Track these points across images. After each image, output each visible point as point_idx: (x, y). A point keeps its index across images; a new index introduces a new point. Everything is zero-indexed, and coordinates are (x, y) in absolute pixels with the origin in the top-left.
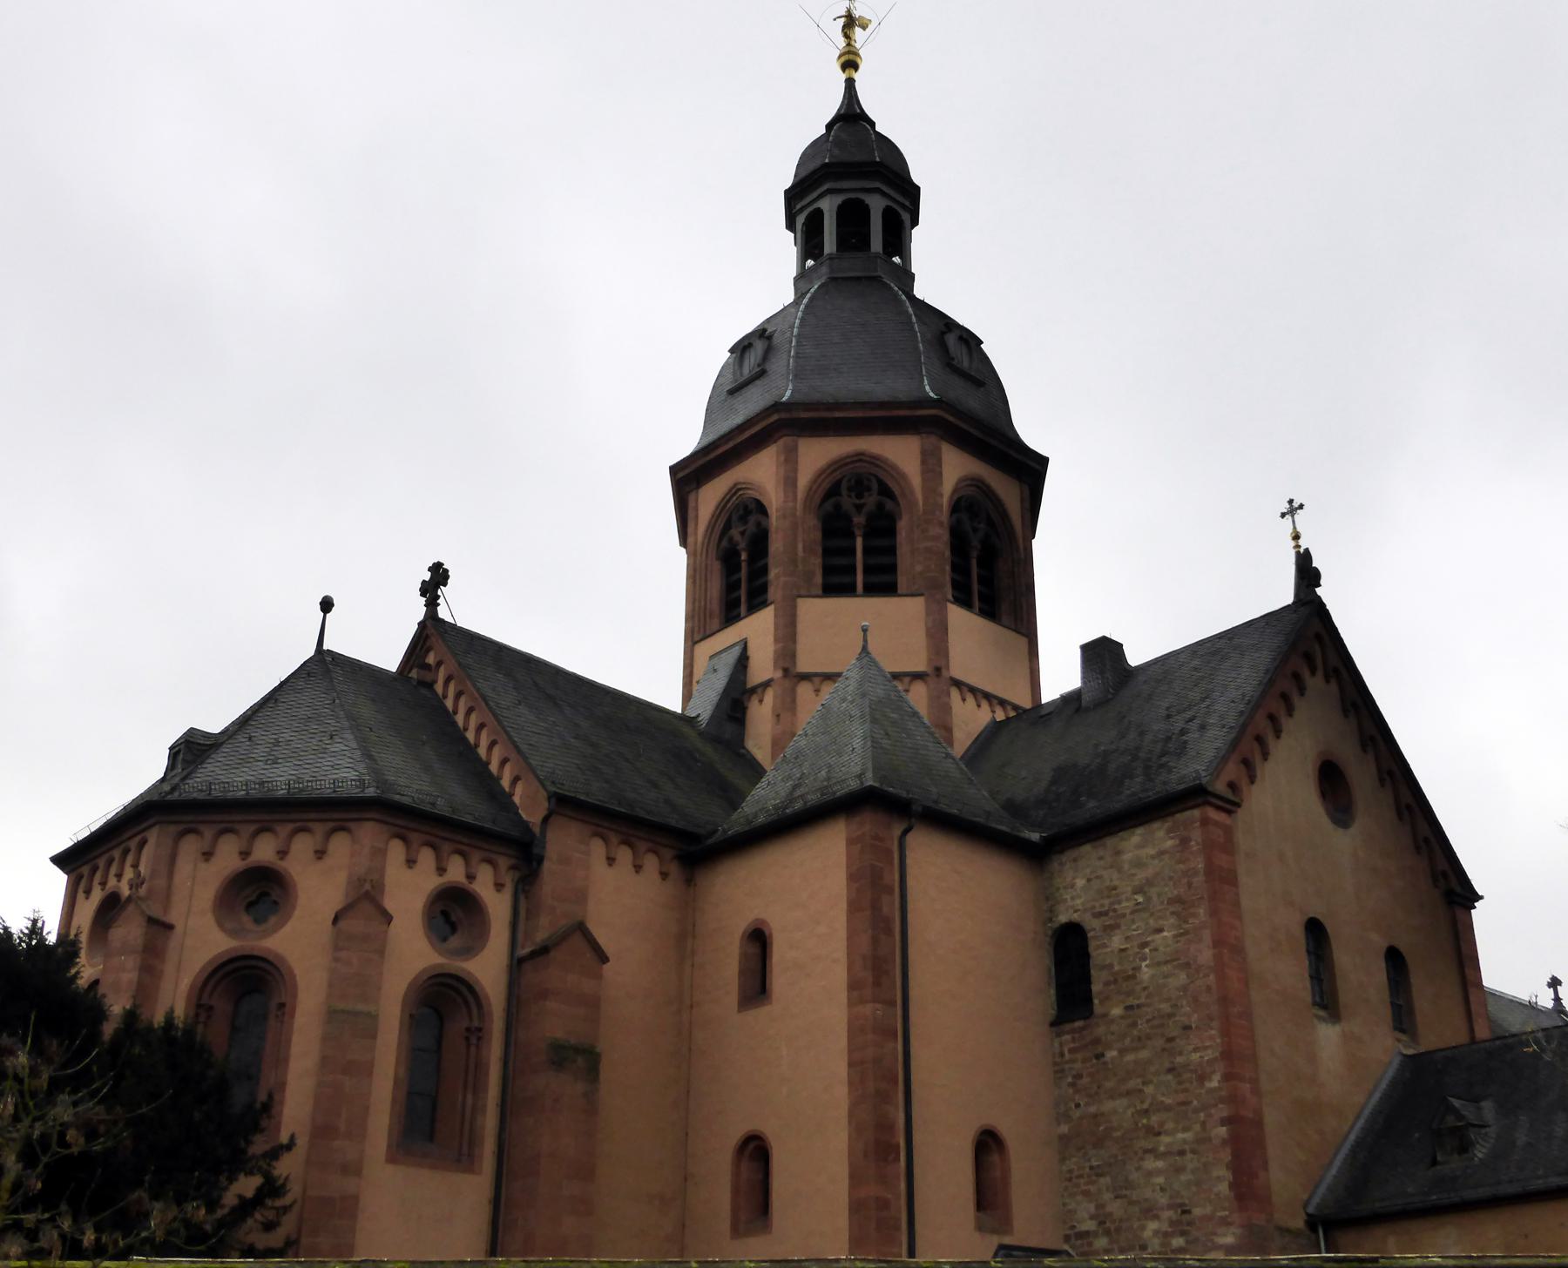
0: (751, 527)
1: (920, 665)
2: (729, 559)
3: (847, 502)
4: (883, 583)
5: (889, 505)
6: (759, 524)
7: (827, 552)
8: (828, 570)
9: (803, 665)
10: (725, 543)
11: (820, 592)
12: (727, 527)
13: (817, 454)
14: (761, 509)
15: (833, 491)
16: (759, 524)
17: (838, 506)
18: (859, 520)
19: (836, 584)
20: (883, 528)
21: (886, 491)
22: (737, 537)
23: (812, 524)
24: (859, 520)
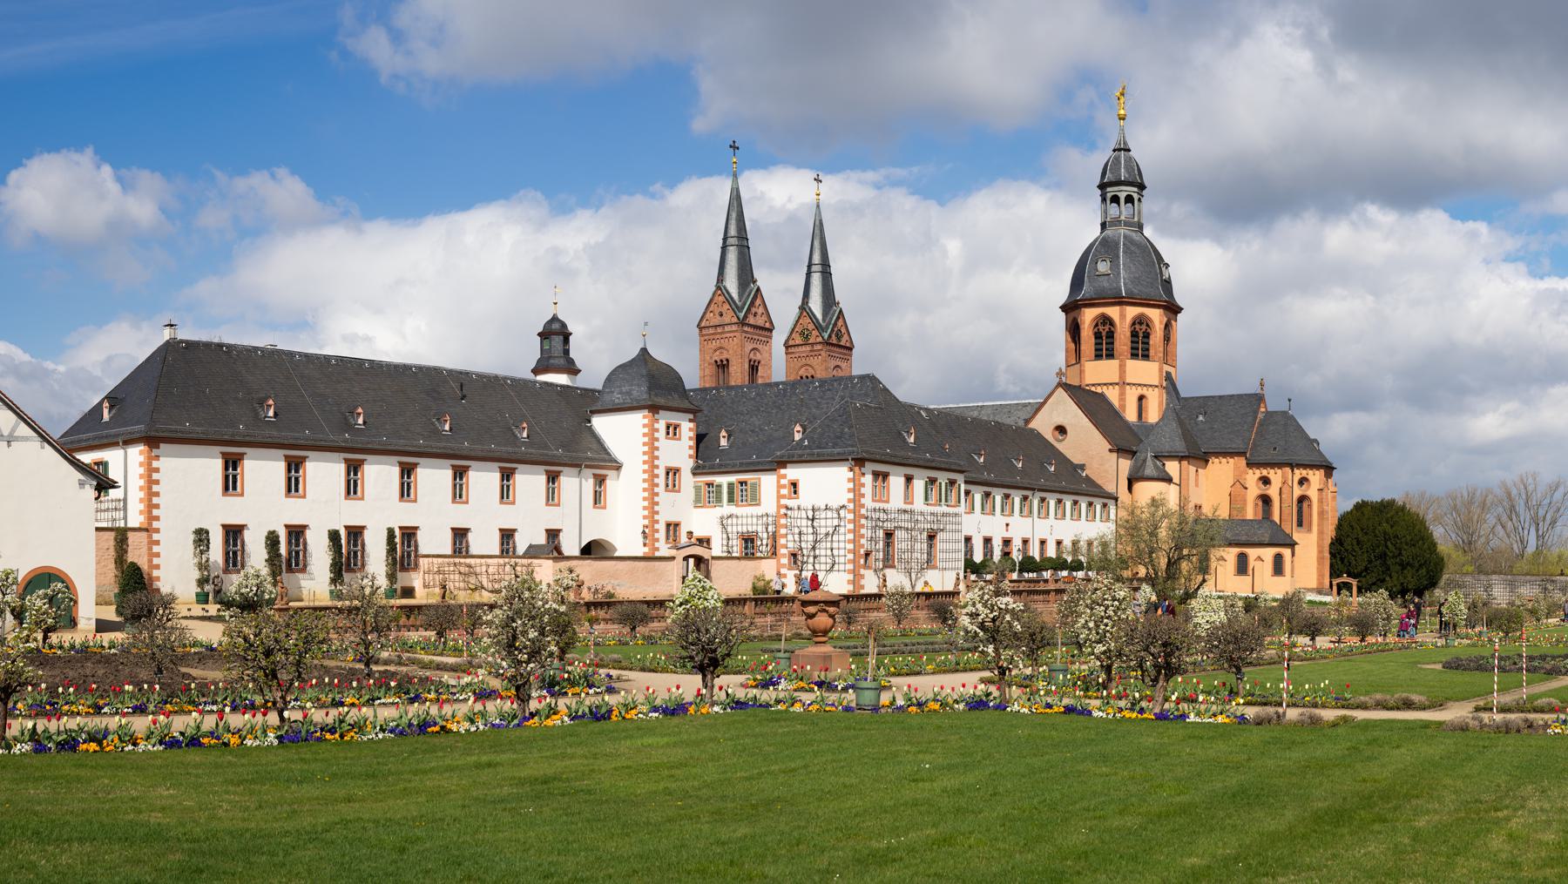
0: (1107, 328)
1: (1157, 384)
2: (1098, 336)
3: (1137, 327)
4: (1146, 357)
5: (1149, 330)
6: (1110, 329)
7: (1132, 342)
8: (1132, 348)
9: (1128, 381)
10: (1096, 330)
11: (1129, 355)
12: (1097, 325)
13: (1132, 312)
14: (1112, 323)
15: (1134, 324)
16: (1110, 329)
17: (1135, 328)
18: (1141, 335)
19: (1134, 356)
20: (1147, 336)
21: (1147, 325)
22: (1101, 330)
23: (1129, 334)
24: (1141, 335)
